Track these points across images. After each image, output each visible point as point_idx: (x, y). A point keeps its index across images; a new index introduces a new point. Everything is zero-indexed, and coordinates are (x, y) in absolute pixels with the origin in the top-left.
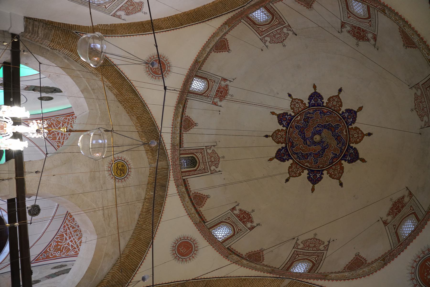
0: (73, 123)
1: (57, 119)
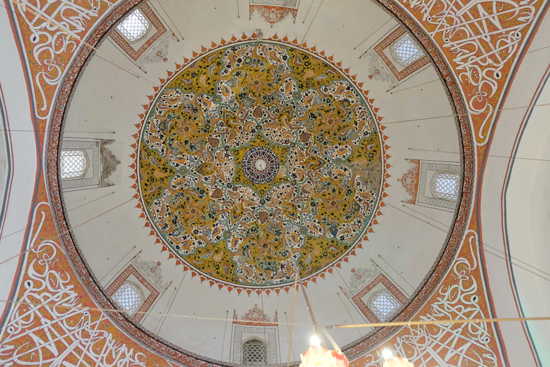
0: (476, 63)
1: (521, 26)
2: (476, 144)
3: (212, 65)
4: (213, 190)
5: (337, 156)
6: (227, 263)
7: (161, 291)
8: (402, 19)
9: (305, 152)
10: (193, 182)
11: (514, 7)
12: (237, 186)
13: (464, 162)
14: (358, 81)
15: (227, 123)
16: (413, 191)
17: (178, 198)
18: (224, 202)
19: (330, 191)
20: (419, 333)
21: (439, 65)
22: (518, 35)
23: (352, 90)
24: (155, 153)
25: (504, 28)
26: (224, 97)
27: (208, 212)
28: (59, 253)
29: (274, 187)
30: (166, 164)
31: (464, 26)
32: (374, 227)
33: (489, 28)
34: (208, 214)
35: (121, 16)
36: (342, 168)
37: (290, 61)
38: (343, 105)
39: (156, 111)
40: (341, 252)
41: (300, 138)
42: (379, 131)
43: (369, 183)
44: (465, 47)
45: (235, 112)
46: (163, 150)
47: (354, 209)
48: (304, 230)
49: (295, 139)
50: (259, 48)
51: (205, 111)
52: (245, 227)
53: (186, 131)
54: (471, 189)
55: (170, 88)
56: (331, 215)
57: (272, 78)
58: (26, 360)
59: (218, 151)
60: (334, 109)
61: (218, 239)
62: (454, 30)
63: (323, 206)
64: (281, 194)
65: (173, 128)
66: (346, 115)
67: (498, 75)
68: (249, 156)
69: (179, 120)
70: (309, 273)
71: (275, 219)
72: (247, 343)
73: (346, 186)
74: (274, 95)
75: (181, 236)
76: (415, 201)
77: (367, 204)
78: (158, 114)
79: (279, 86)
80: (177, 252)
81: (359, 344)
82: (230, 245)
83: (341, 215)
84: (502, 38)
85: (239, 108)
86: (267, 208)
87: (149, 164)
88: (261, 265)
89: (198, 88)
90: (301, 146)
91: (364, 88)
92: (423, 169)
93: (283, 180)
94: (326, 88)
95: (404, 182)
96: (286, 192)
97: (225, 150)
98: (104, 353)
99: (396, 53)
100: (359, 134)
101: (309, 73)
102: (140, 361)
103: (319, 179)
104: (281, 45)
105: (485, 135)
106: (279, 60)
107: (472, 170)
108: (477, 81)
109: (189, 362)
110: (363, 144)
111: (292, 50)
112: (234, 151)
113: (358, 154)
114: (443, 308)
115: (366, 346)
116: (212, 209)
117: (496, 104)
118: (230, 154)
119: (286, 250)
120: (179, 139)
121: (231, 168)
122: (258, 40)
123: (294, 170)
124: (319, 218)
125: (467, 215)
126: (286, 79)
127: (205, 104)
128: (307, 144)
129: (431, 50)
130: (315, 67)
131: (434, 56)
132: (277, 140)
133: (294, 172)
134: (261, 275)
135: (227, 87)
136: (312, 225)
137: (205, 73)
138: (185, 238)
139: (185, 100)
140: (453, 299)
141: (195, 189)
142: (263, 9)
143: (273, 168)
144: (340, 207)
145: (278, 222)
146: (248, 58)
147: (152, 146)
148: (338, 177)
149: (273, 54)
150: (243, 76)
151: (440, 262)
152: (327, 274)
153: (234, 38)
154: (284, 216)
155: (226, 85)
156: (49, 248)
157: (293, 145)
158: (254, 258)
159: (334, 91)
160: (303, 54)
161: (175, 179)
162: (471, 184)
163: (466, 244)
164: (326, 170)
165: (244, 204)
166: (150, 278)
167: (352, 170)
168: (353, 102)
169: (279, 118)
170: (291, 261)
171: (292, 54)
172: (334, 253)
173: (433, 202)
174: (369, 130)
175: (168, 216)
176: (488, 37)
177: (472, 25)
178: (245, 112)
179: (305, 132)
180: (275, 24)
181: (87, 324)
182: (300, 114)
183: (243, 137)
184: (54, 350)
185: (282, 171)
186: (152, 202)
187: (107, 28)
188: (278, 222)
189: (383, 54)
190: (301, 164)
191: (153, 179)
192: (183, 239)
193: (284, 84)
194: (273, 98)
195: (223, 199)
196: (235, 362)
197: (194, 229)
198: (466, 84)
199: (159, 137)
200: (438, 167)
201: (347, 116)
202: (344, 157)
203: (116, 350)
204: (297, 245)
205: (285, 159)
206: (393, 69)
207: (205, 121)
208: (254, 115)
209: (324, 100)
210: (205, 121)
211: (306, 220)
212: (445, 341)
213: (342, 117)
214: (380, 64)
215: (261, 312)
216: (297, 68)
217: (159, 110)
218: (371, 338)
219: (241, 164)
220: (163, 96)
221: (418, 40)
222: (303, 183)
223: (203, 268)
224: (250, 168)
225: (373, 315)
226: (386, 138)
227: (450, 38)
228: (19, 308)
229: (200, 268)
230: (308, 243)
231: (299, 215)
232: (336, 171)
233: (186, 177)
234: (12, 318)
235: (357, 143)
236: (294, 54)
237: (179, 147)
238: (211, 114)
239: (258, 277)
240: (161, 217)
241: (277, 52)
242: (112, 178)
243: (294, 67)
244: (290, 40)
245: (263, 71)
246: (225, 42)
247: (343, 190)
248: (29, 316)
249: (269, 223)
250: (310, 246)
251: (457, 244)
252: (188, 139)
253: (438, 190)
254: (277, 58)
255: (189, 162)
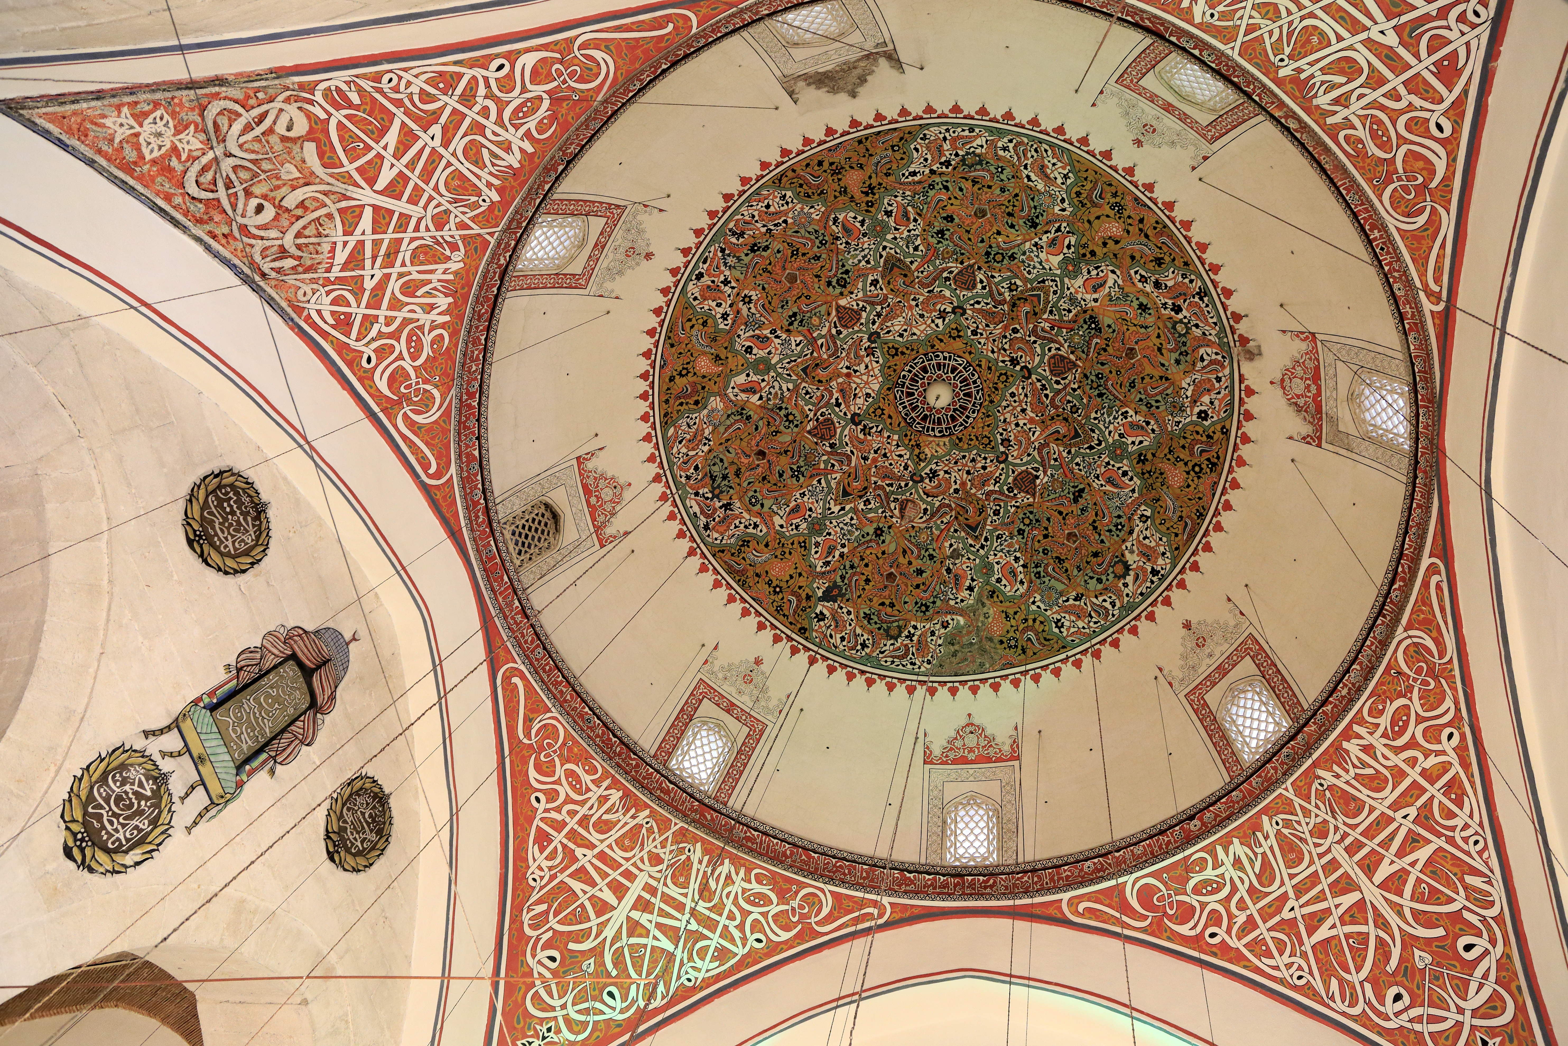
0: (1234, 889)
1: (1319, 985)
2: (1065, 896)
3: (1153, 247)
4: (854, 303)
5: (998, 563)
6: (700, 388)
7: (592, 288)
8: (1318, 717)
9: (991, 488)
10: (860, 258)
11: (1358, 969)
12: (878, 353)
13: (1025, 872)
14: (1176, 595)
15: (1019, 299)
16: (952, 755)
17: (813, 237)
18: (832, 336)
19: (917, 564)
20: (667, 850)
21: (1226, 803)
22: (1300, 978)
23: (1152, 582)
24: (902, 159)
25: (1313, 947)
26: (1079, 282)
27: (800, 309)
28: (591, 93)
29: (896, 437)
30: (882, 190)
31: (1312, 862)
32: (860, 680)
33: (1312, 915)
34: (796, 310)
35: (1213, 65)
36: (973, 580)
37: (1198, 428)
38: (1116, 563)
39: (1006, 140)
40: (791, 623)
41: (1022, 472)
42: (1070, 653)
43: (952, 648)
44: (1266, 864)
45: (1051, 312)
46: (914, 174)
47: (889, 628)
48: (817, 527)
49: (1018, 461)
50: (1217, 354)
51: (1036, 245)
52: (790, 399)
53: (975, 214)
54: (971, 895)
55: (1070, 158)
56: (864, 578)
57: (1149, 388)
58: (341, 139)
59: (947, 293)
60: (1102, 541)
61: (746, 351)
62: (1301, 839)
63: (880, 555)
64: (885, 455)
65: (975, 182)
66: (1094, 571)
67: (1213, 935)
68: (954, 363)
69: (998, 192)
70: (730, 566)
71: (825, 458)
72: (547, 506)
73: (936, 597)
74: (1111, 397)
75: (727, 273)
76: (931, 763)
77: (905, 655)
78: (1000, 144)
79: (1133, 406)
80: (689, 279)
81: (615, 736)
82: (741, 379)
83: (871, 600)
84: (1293, 945)
85: (1062, 320)
86: (845, 432)
87: (871, 155)
88: (718, 461)
89: (1089, 222)
90: (1003, 477)
91: (1160, 611)
92: (1001, 770)
93: (917, 451)
94: (1148, 518)
95: (968, 729)
96: (891, 464)
97: (954, 309)
98: (419, 272)
99: (1245, 692)
100: (1056, 608)
101: (1176, 476)
102: (433, 343)
103: (937, 533)
104: (1231, 404)
105: (1086, 913)
106: (1195, 402)
107: (1010, 893)
108: (1196, 891)
109: (466, 428)
110: (1034, 620)
111: (1226, 432)
112: (956, 329)
113: (1011, 612)
114: (725, 885)
115: (615, 752)
116: (808, 315)
117: (1152, 934)
118: (947, 320)
119: (765, 502)
120: (953, 201)
121: (915, 330)
122: (1235, 352)
123: (946, 472)
124: (852, 551)
125: (915, 893)
126: (1152, 422)
127: (1052, 243)
128: (1010, 490)
129: (1254, 784)
130: (1192, 488)
131: (1241, 791)
132: (1005, 421)
133: (942, 473)
134: (696, 468)
135: (1107, 286)
136: (833, 543)
137: (1128, 232)
138: (726, 282)
139: (1051, 195)
140: (748, 901)
141: (843, 266)
142: (1310, 365)
143: (939, 423)
144: (887, 593)
145: (822, 466)
146: (1188, 329)
147: (917, 150)
148: (951, 575)
149: (1207, 386)
150: (1140, 320)
151: (815, 853)
152: (738, 607)
153: (1228, 293)
154: (838, 476)
155: (1110, 283)
156: (595, 70)
157: (1003, 459)
158: (728, 440)
159: (1144, 538)
160: (1218, 458)
161: (855, 218)
162: (982, 895)
163: (862, 904)
164: (961, 545)
165: (840, 380)
166: (611, 255)
167: (972, 606)
168: (1126, 585)
169: (1058, 416)
170: (743, 521)
171: (1214, 433)
172: (786, 606)
173: (935, 806)
174: (1068, 630)
175: (764, 230)
176: (1291, 915)
177: (1314, 879)
178: (1057, 335)
179: (1038, 481)
180: (1280, 392)
181: (464, 213)
182: (1077, 464)
183: (994, 341)
184: (385, 178)
185: (938, 445)
186: (785, 189)
187: (1173, 39)
188: (822, 466)
189: (1243, 658)
190: (963, 484)
191: (840, 173)
192: (722, 278)
193: (1139, 418)
194: (1100, 395)
195: (839, 333)
196: (499, 507)
197: (753, 293)
198: (1188, 867)
199: (943, 159)
200: (1009, 806)
201: (1091, 574)
202: (999, 581)
203: (435, 289)
204: (782, 522)
205: (966, 446)
206: (1211, 681)
207: (1011, 248)
208: (1053, 357)
209: (1119, 517)
210: (1011, 248)
211: (841, 525)
212: (665, 902)
213: (1088, 563)
214: (1220, 650)
215: (617, 500)
216: (1183, 447)
217: (1011, 145)
218: (633, 756)
219: (929, 349)
220: (1047, 148)
221: (1274, 754)
222: (922, 500)
223: (672, 346)
224: (926, 372)
225: (678, 739)
226: (1057, 672)
227: (1284, 830)
228: (441, 74)
229: (670, 338)
230: (792, 544)
231: (848, 507)
232: (964, 567)
233: (866, 239)
234: (415, 72)
235: (1034, 607)
236: (1216, 437)
237: (933, 205)
238: (1032, 260)
239: (689, 464)
240: (757, 218)
241: (1213, 396)
242: (810, 94)
243: (1185, 438)
244: (1249, 428)
245: (1163, 365)
246: (1216, 274)
247: (925, 591)
248: (433, 99)
249: (813, 446)
250: (787, 551)
251: (858, 884)
252: (957, 220)
253: (962, 813)
254: (1200, 396)
255: (904, 236)
